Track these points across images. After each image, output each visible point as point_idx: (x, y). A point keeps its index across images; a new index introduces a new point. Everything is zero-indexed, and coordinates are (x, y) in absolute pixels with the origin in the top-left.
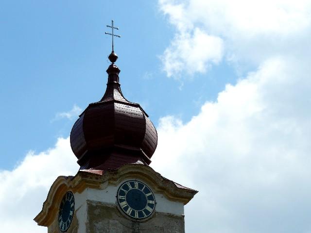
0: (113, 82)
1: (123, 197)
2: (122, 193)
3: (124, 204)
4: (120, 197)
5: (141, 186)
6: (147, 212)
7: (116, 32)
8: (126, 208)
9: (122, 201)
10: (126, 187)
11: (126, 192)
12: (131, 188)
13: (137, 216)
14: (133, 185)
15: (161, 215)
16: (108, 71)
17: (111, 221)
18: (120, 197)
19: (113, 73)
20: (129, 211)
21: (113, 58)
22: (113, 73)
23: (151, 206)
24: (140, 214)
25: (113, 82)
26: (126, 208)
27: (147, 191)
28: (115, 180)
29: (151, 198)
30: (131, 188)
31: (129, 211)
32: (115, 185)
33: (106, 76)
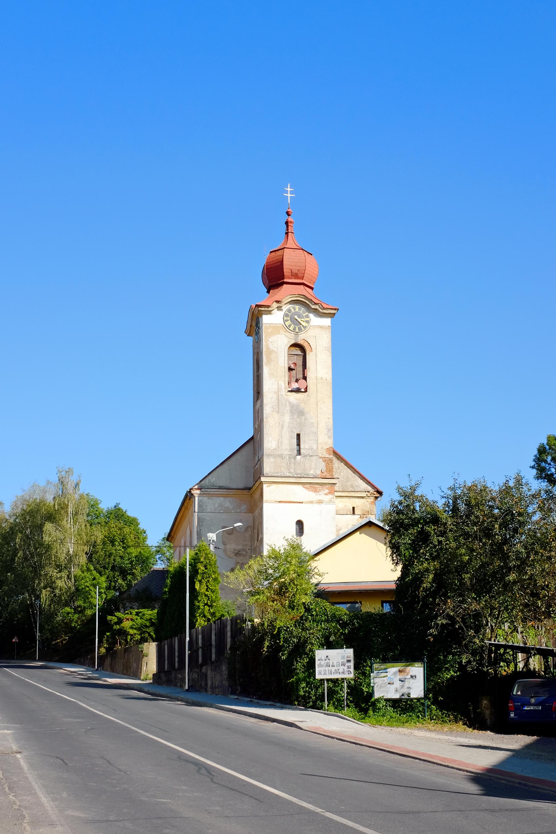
1: (289, 318)
4: (285, 318)
6: (305, 327)
8: (290, 326)
11: (290, 314)
12: (293, 311)
13: (297, 330)
15: (315, 326)
17: (279, 335)
18: (285, 318)
20: (291, 328)
23: (308, 322)
24: (300, 329)
26: (290, 326)
29: (307, 316)
30: (293, 311)
31: (291, 328)
32: (282, 310)
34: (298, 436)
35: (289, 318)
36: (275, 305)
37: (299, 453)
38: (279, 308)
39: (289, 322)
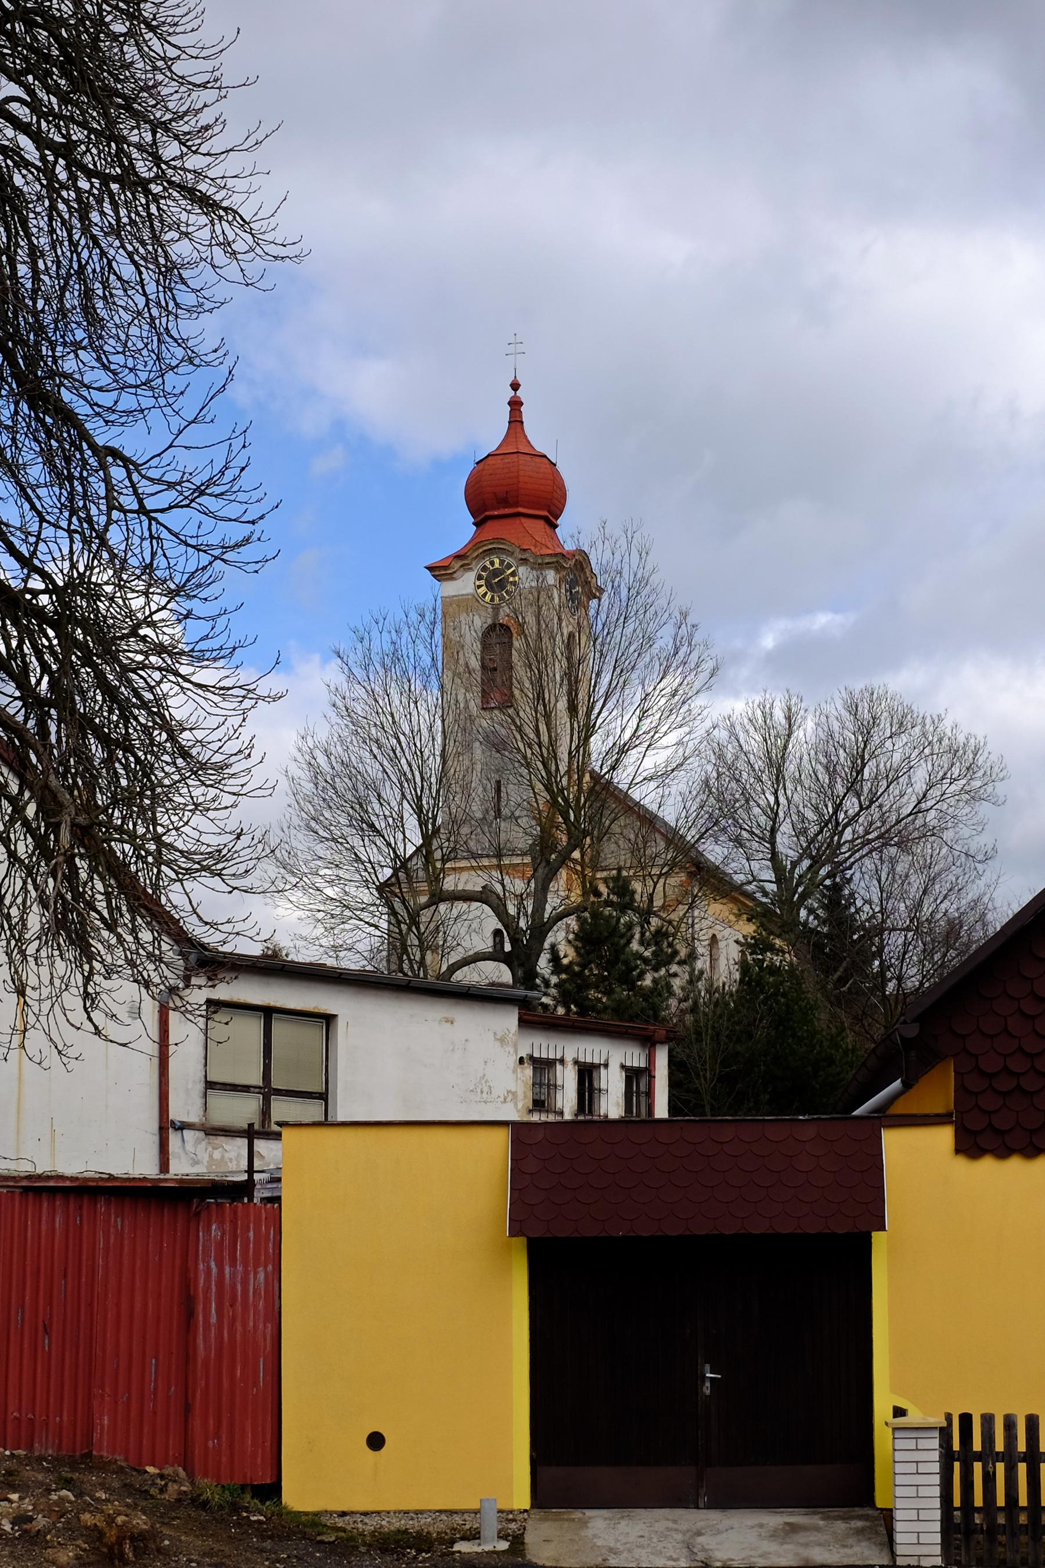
0: (516, 420)
1: (482, 582)
2: (480, 578)
3: (483, 590)
4: (478, 583)
5: (502, 562)
7: (520, 348)
9: (479, 587)
10: (484, 569)
13: (497, 599)
14: (492, 563)
16: (509, 403)
18: (478, 583)
19: (515, 405)
20: (488, 598)
21: (515, 386)
22: (515, 405)
24: (502, 598)
25: (516, 420)
27: (509, 566)
28: (468, 564)
31: (488, 598)
33: (505, 412)
34: (498, 783)
35: (482, 582)
36: (457, 565)
37: (498, 814)
38: (466, 568)
39: (484, 588)
